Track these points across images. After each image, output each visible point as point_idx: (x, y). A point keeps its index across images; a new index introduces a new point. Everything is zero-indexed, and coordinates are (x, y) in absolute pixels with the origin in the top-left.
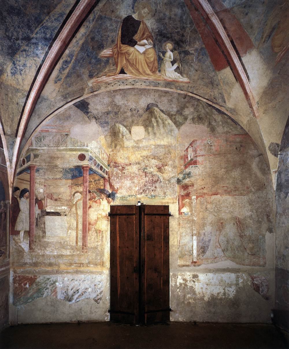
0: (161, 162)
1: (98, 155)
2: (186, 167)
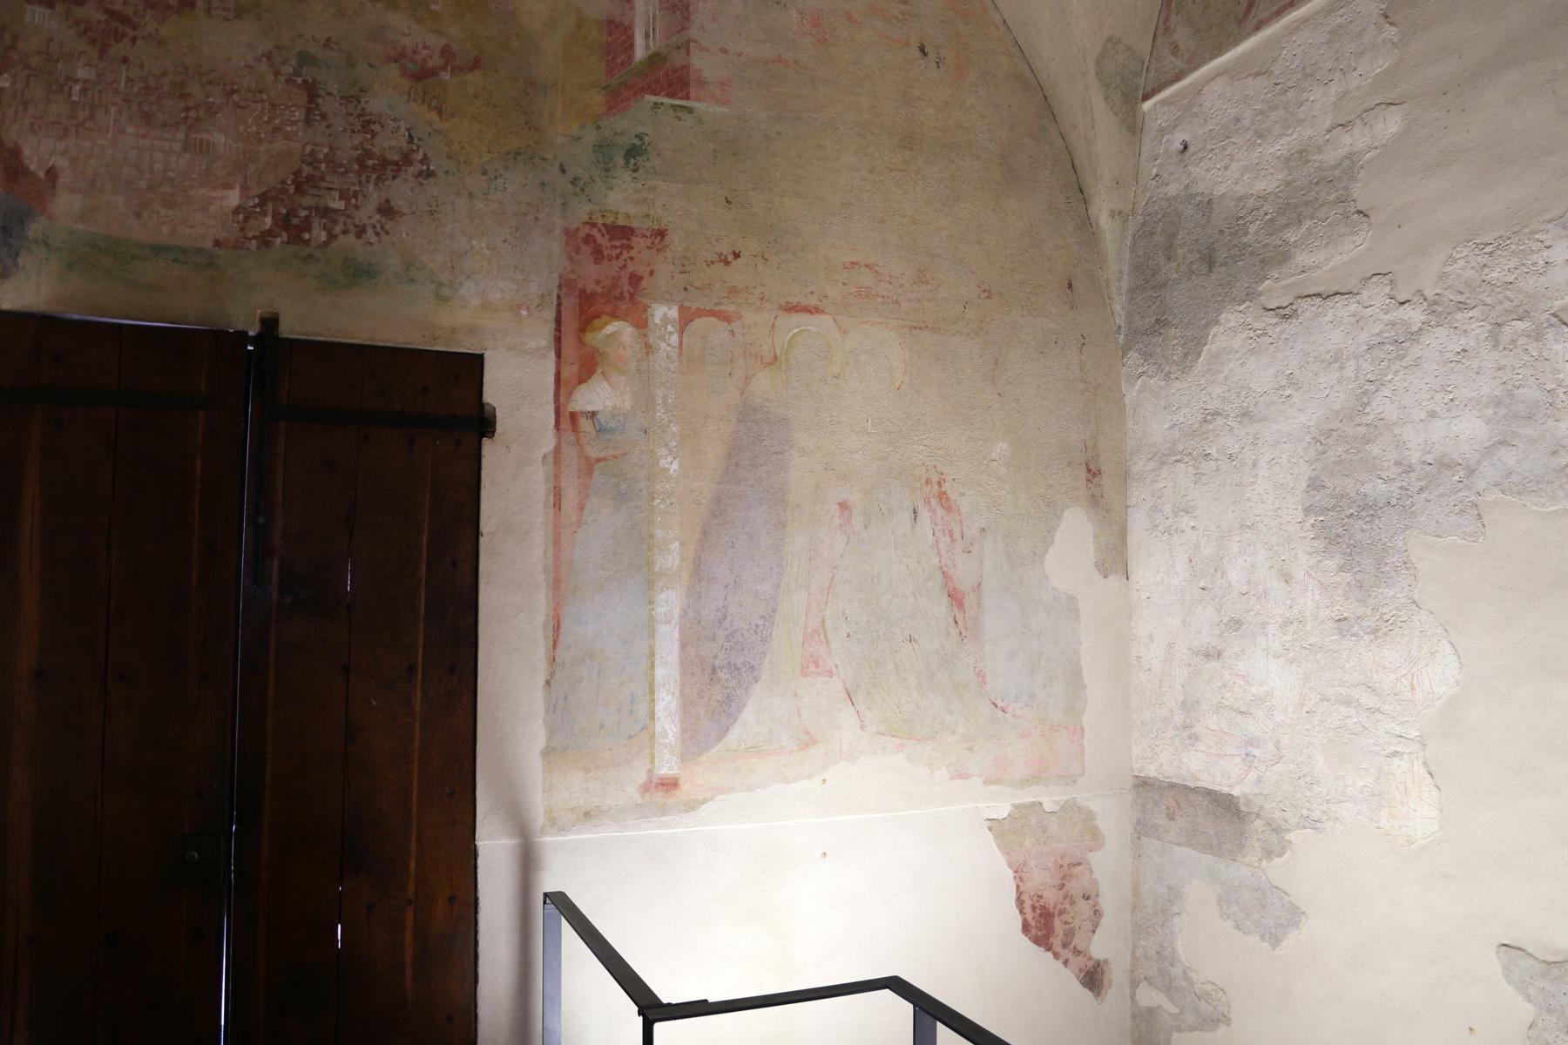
2: (617, 99)
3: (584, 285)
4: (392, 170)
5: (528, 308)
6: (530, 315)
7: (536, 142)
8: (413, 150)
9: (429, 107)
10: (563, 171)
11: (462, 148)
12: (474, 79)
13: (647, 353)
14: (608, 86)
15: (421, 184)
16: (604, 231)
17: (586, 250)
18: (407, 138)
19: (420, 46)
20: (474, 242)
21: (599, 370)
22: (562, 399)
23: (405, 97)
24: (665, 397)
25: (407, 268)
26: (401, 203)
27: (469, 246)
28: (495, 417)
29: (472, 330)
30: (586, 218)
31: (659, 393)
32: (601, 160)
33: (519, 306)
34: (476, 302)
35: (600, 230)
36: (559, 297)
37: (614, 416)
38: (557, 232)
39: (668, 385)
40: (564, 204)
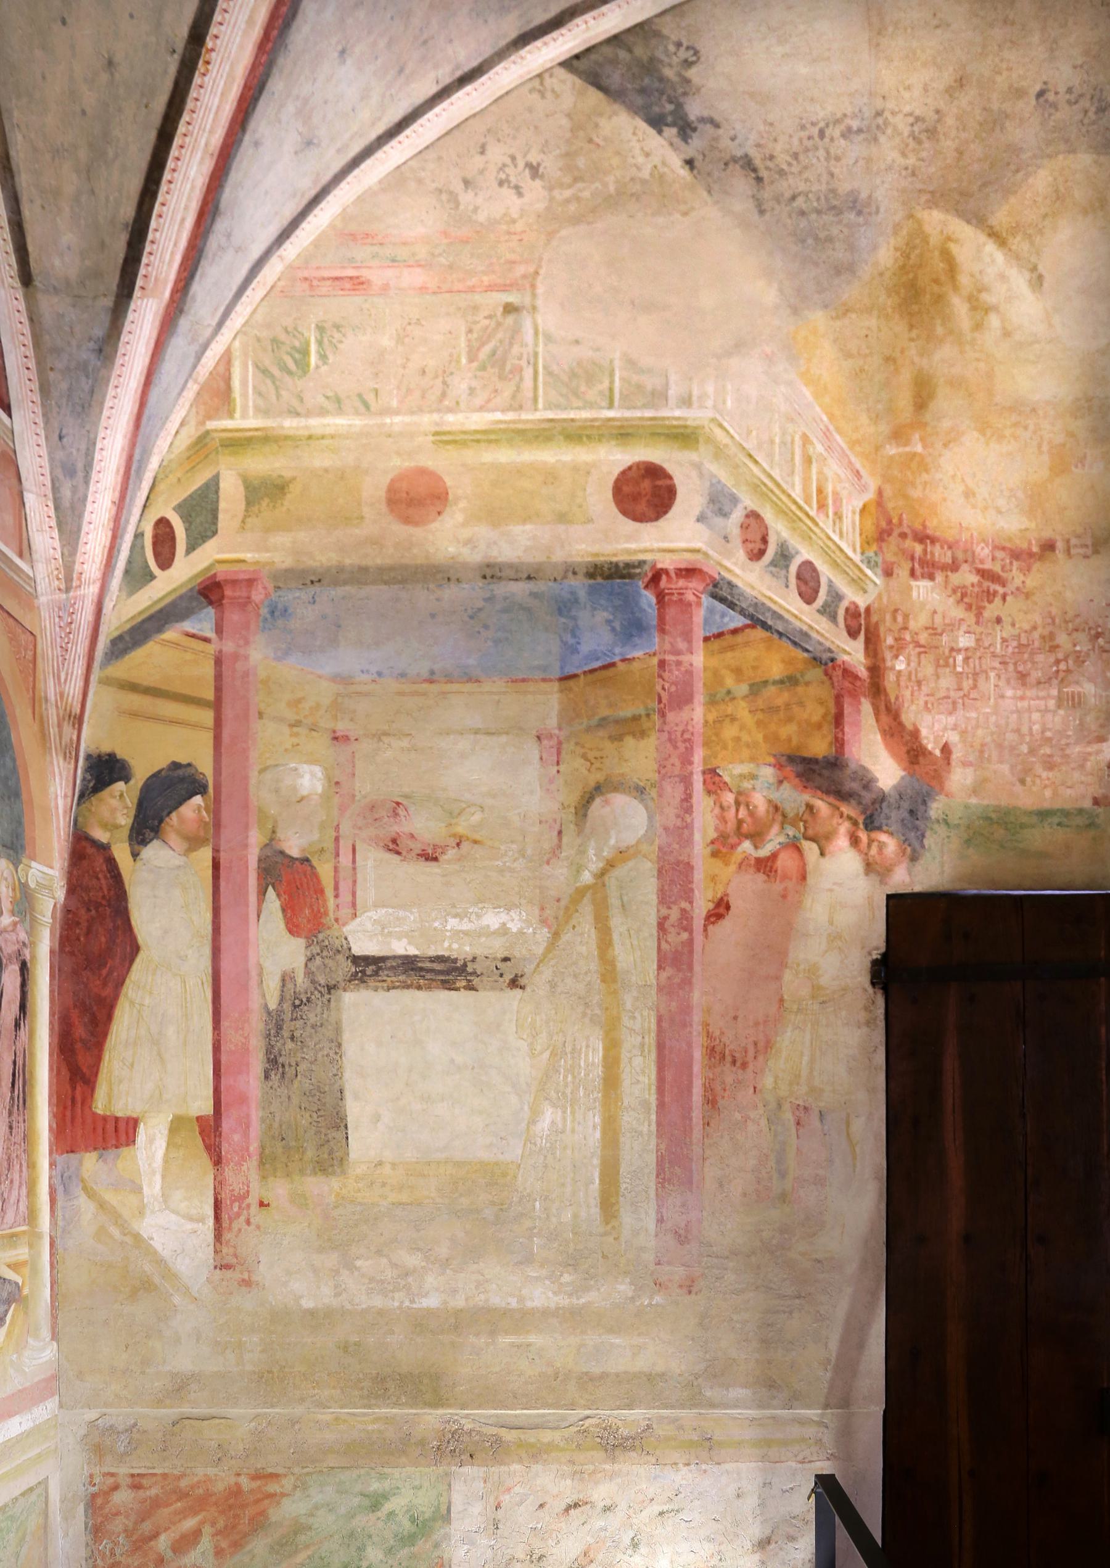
1: (776, 474)
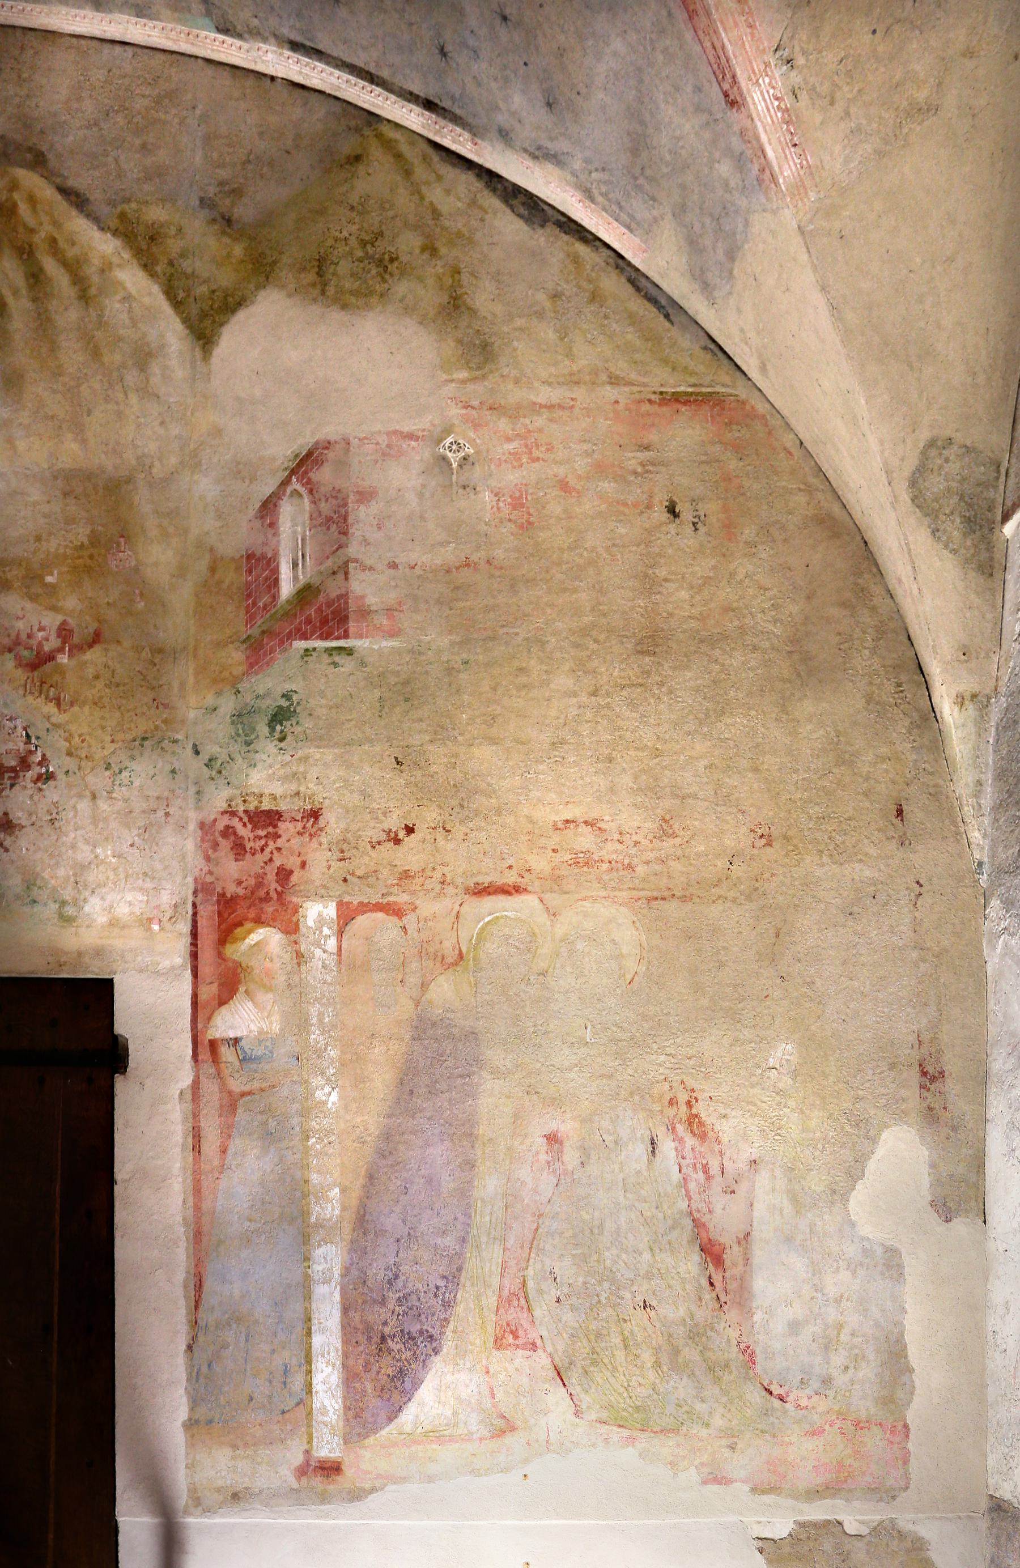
0: (54, 609)
3: (223, 888)
4: (10, 778)
5: (160, 921)
6: (162, 929)
7: (165, 722)
8: (31, 752)
9: (46, 698)
10: (197, 753)
11: (83, 741)
12: (94, 656)
13: (299, 964)
14: (249, 637)
15: (40, 790)
16: (246, 819)
17: (225, 844)
18: (24, 738)
19: (35, 628)
20: (99, 851)
21: (242, 989)
22: (200, 1026)
23: (21, 692)
24: (321, 1015)
25: (28, 888)
26: (20, 814)
27: (93, 856)
28: (127, 1049)
29: (99, 952)
30: (224, 806)
31: (314, 1011)
32: (241, 731)
33: (150, 920)
34: (102, 919)
35: (241, 819)
36: (194, 905)
37: (260, 1042)
38: (192, 826)
39: (324, 1000)
40: (198, 793)
